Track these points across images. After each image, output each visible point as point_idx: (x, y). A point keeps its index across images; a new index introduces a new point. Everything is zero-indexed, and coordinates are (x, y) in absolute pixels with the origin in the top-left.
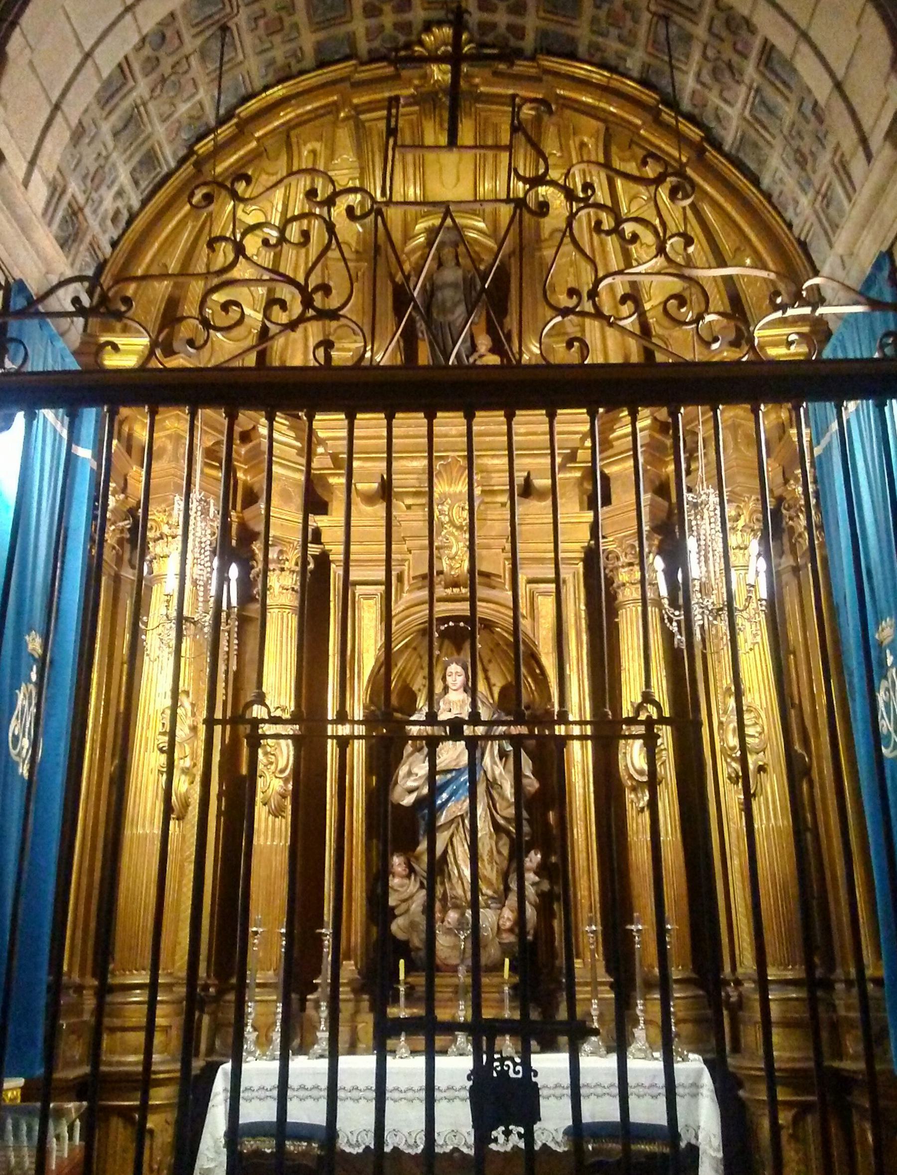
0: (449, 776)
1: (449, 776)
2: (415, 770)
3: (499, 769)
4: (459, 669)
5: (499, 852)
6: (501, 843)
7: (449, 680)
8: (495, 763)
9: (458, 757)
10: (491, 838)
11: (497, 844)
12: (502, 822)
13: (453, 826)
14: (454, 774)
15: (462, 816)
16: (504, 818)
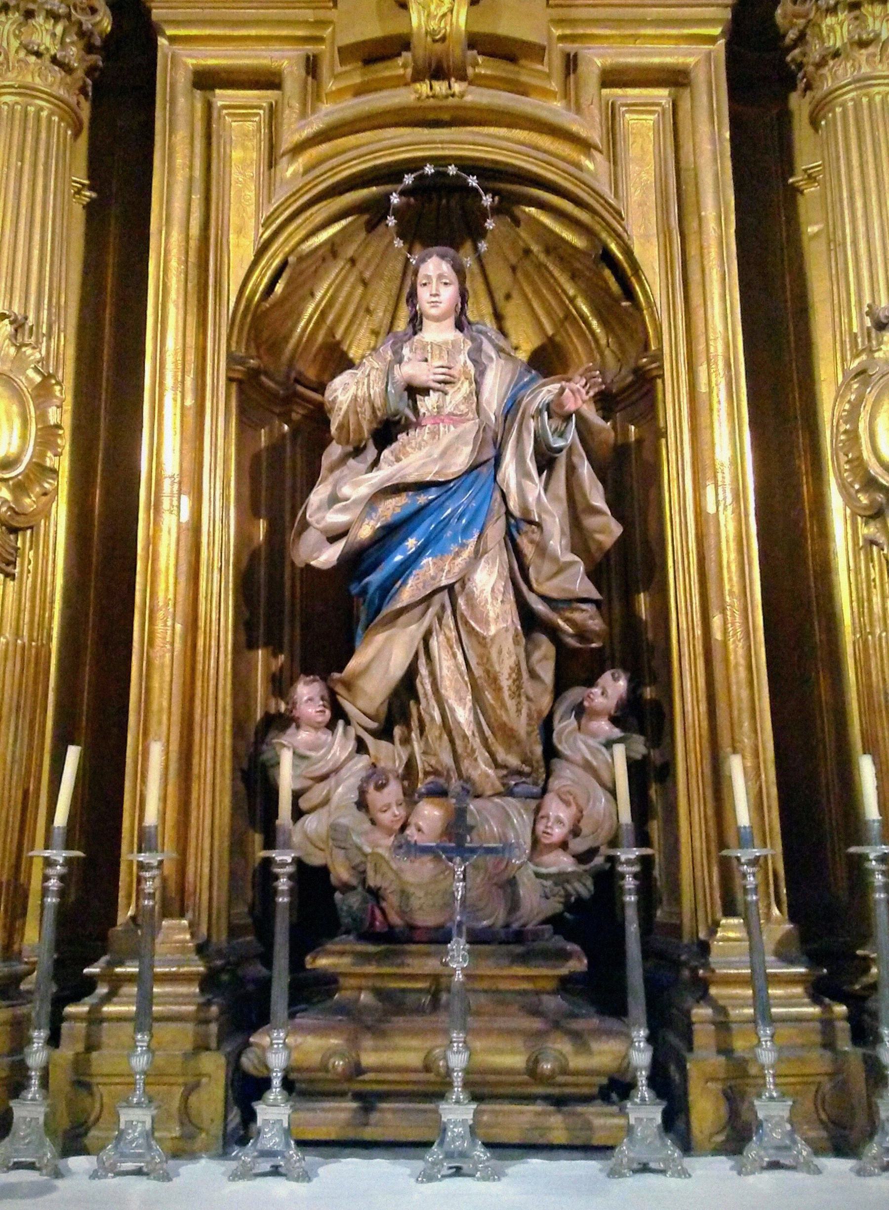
0: (422, 499)
1: (422, 499)
2: (346, 490)
3: (535, 489)
4: (446, 267)
5: (534, 675)
6: (537, 656)
7: (424, 294)
8: (527, 475)
9: (443, 454)
10: (516, 642)
11: (528, 656)
12: (540, 607)
13: (432, 611)
14: (432, 494)
15: (450, 588)
16: (545, 598)
